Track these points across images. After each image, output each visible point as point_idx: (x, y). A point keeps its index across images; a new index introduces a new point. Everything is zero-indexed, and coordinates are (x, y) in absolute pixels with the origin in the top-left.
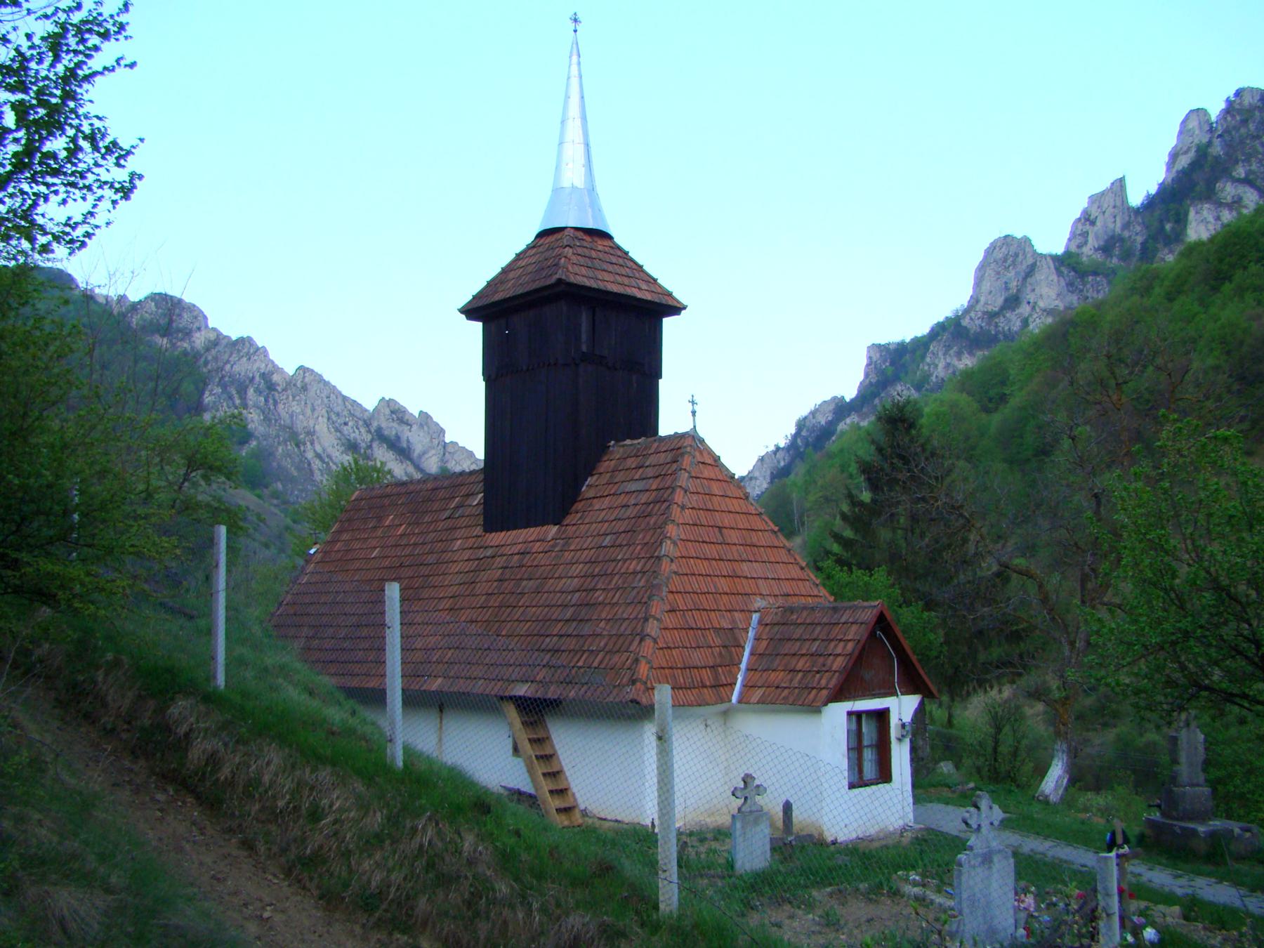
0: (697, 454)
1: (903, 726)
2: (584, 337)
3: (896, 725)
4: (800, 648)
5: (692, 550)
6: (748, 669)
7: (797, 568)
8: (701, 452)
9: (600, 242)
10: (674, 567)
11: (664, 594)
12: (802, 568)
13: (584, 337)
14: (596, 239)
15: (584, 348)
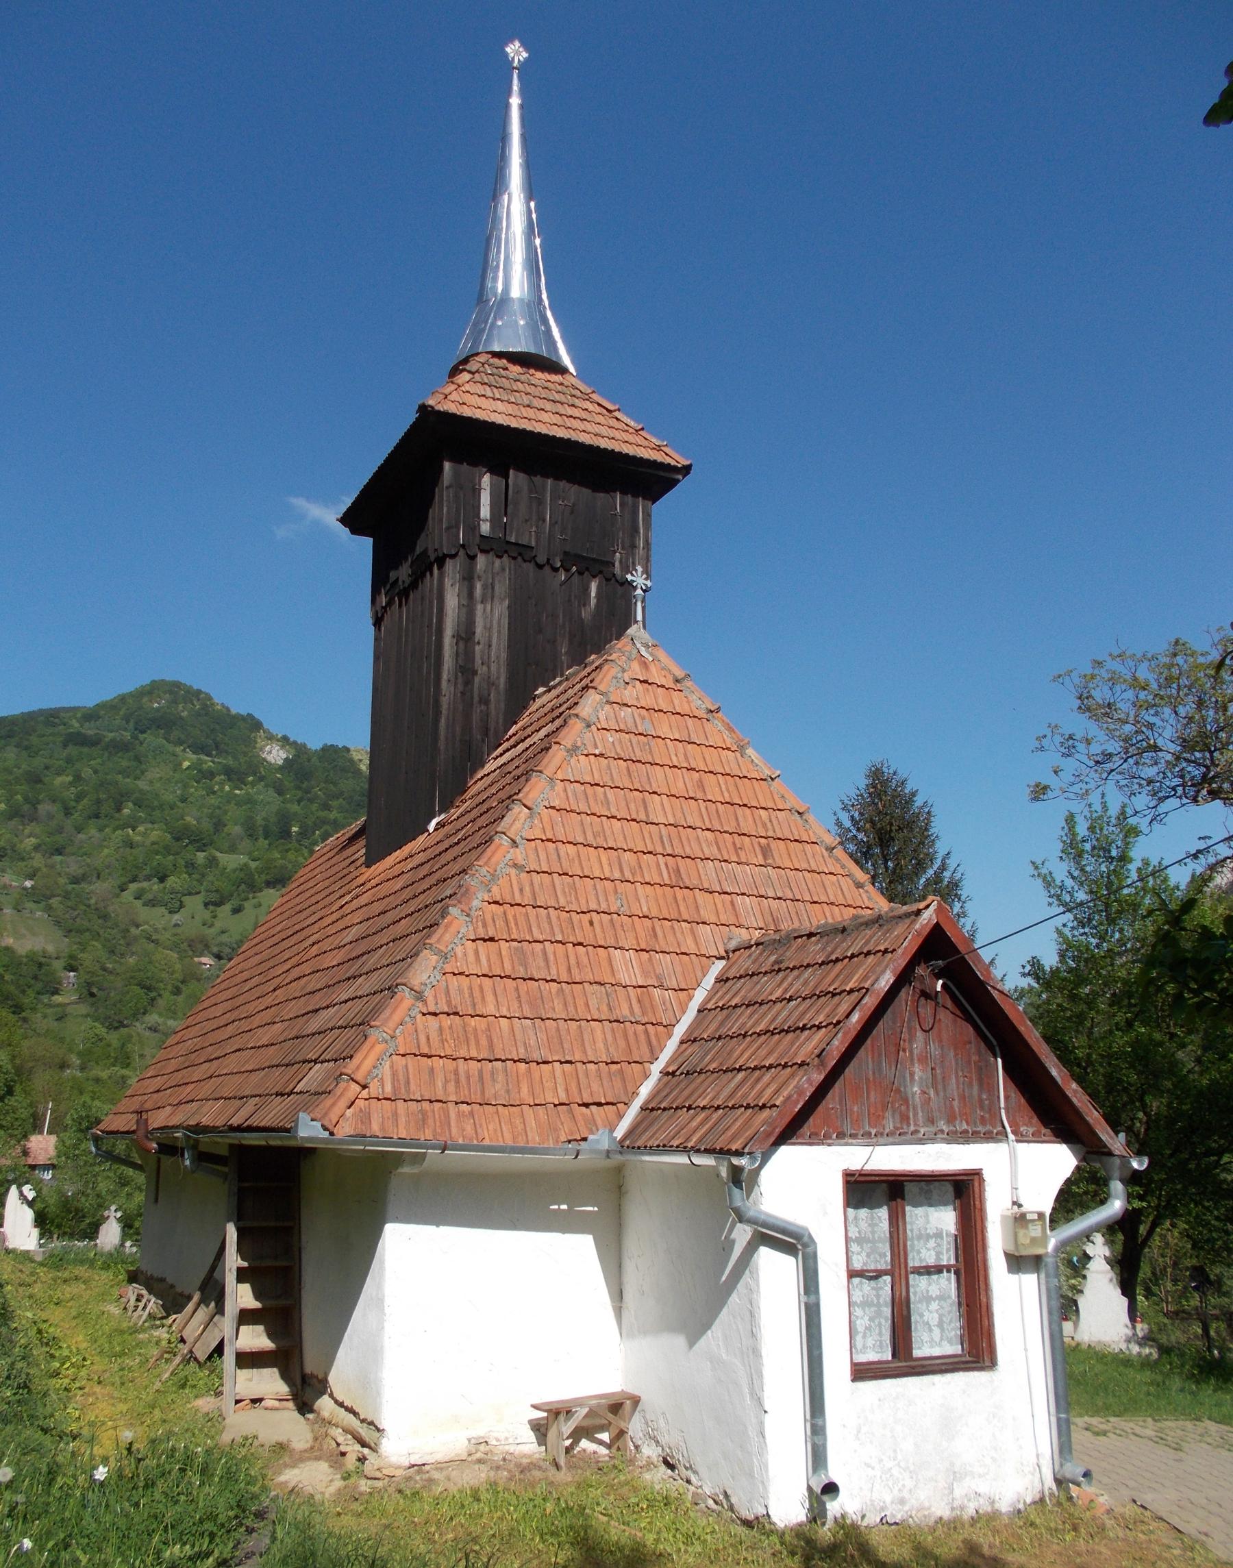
0: (635, 666)
1: (1020, 1220)
2: (485, 511)
3: (1004, 1218)
4: (757, 1023)
5: (571, 827)
6: (665, 1073)
7: (846, 883)
8: (644, 665)
9: (539, 375)
10: (519, 855)
11: (476, 903)
12: (859, 886)
13: (485, 511)
14: (532, 371)
15: (485, 528)
